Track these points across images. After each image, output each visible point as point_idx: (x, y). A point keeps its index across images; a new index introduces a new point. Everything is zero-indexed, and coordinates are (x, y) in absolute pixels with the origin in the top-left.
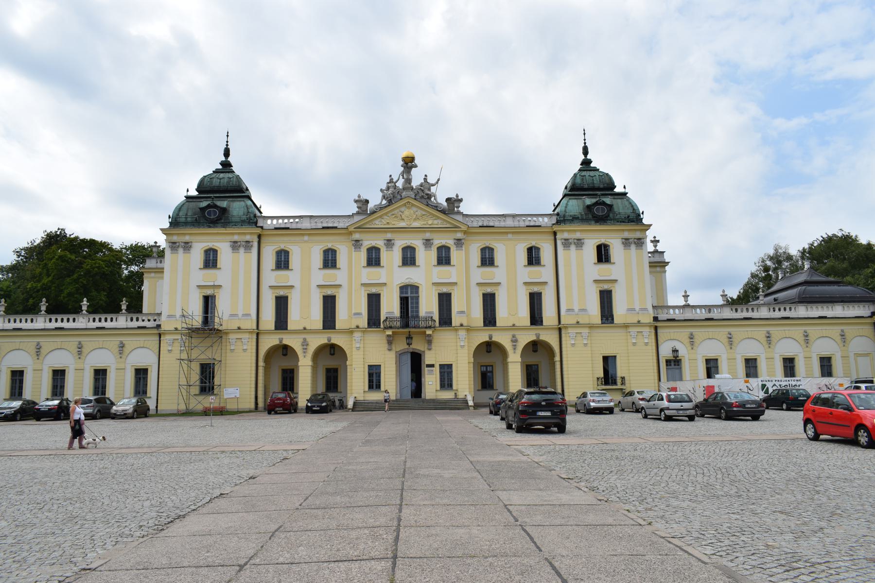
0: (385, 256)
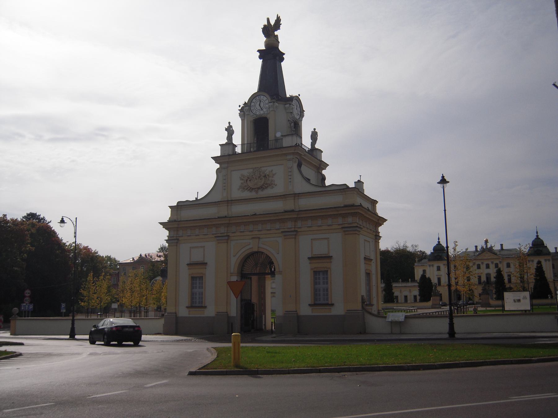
0: (481, 266)
